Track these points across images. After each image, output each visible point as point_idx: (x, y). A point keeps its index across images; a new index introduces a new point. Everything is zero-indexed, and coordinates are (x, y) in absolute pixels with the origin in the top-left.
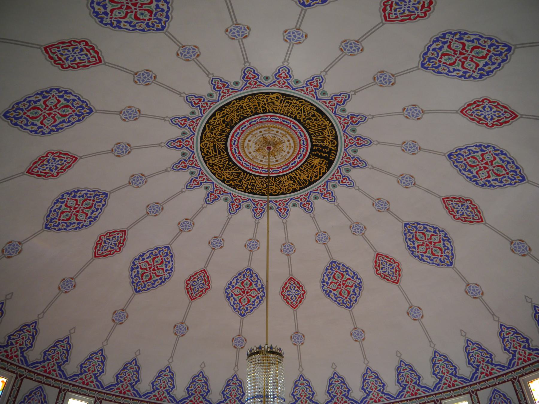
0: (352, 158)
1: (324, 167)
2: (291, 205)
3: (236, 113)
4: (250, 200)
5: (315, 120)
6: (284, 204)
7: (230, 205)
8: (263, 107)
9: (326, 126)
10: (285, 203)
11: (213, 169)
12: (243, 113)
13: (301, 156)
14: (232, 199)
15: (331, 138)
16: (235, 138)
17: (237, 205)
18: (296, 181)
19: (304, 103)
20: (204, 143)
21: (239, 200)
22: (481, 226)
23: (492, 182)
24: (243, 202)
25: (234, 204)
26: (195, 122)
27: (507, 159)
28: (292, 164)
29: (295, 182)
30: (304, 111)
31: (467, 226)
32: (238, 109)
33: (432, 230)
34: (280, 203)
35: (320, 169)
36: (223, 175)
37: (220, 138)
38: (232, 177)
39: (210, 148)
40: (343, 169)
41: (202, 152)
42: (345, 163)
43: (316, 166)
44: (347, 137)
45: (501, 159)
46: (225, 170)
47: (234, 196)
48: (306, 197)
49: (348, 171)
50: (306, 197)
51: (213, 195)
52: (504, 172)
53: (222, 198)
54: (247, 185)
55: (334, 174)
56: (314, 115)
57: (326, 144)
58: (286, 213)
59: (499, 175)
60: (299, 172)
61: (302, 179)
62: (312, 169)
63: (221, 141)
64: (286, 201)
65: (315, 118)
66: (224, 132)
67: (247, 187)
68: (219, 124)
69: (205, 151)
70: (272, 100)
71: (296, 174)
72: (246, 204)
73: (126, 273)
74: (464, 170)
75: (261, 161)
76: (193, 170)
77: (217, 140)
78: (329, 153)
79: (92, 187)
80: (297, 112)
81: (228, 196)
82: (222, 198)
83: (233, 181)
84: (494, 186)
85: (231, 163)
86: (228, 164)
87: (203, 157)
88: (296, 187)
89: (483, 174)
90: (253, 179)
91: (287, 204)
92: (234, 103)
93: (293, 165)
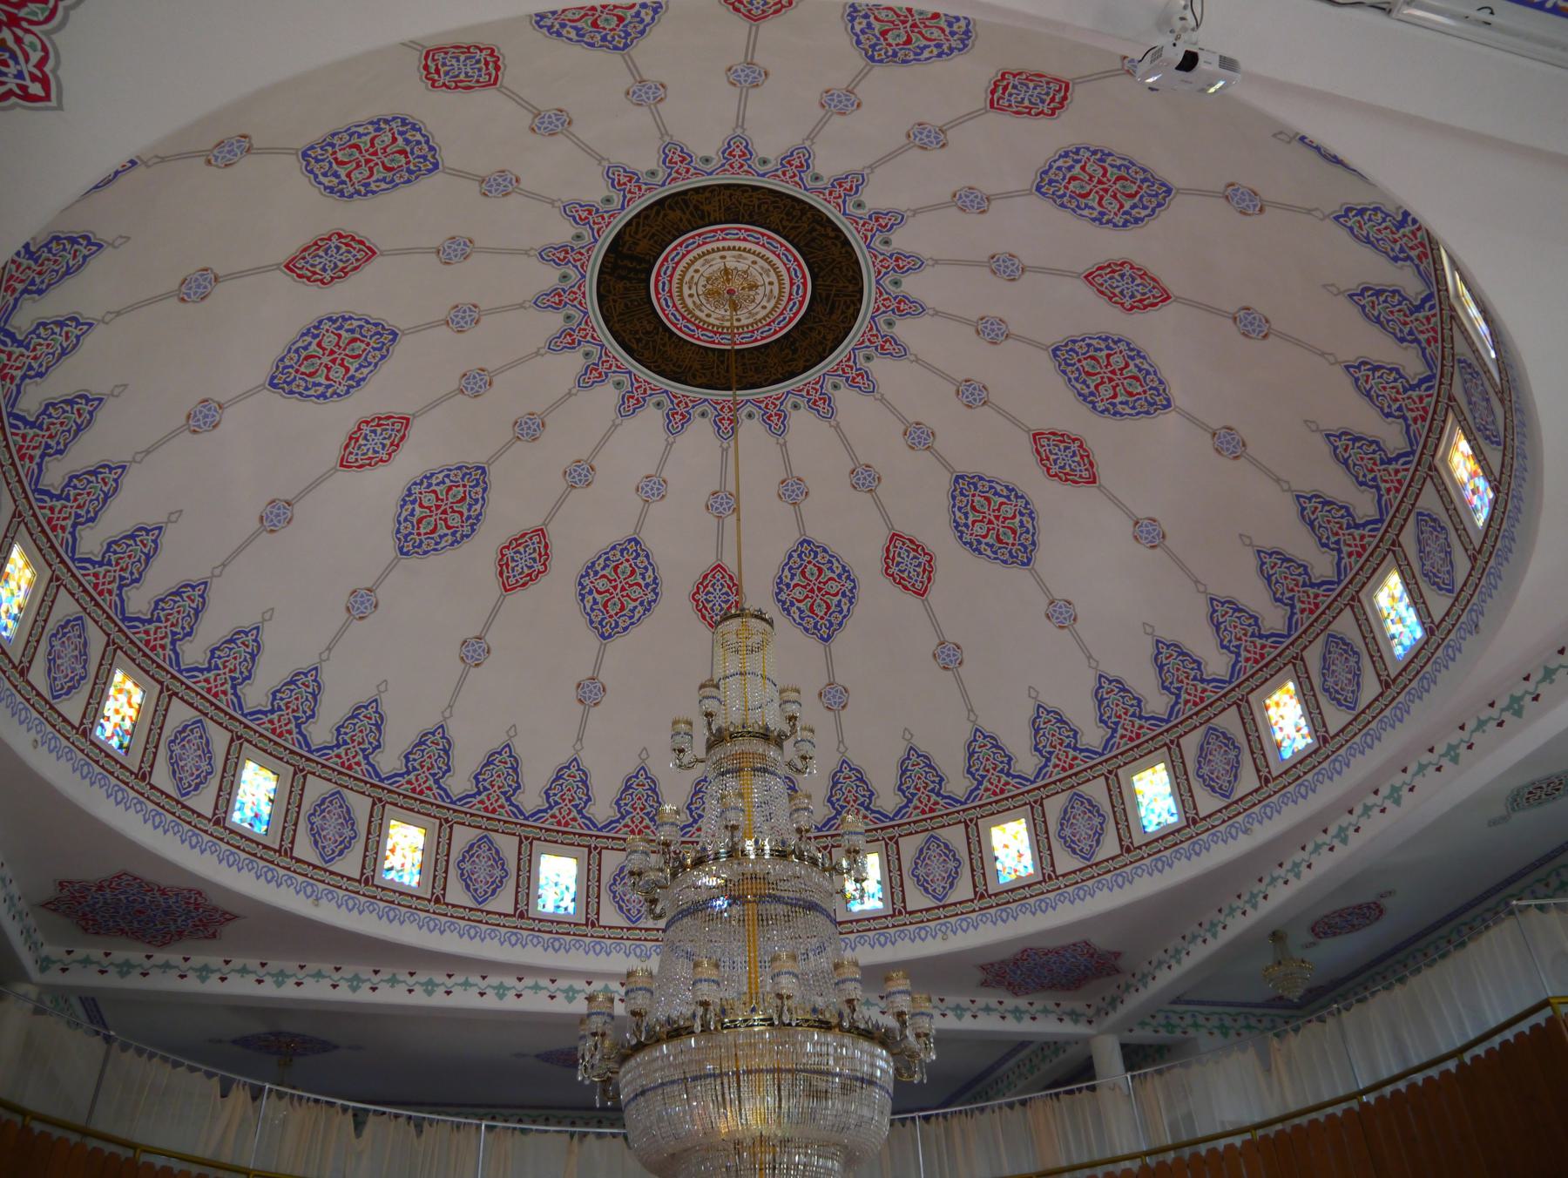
1: (627, 237)
22: (284, 257)
23: (308, 339)
26: (841, 370)
27: (311, 392)
29: (696, 207)
31: (307, 239)
33: (373, 187)
45: (320, 384)
52: (303, 369)
56: (639, 341)
59: (307, 358)
61: (679, 213)
69: (851, 311)
73: (1153, 226)
74: (361, 327)
76: (891, 288)
79: (1060, 381)
81: (850, 209)
83: (826, 236)
84: (304, 335)
89: (329, 341)
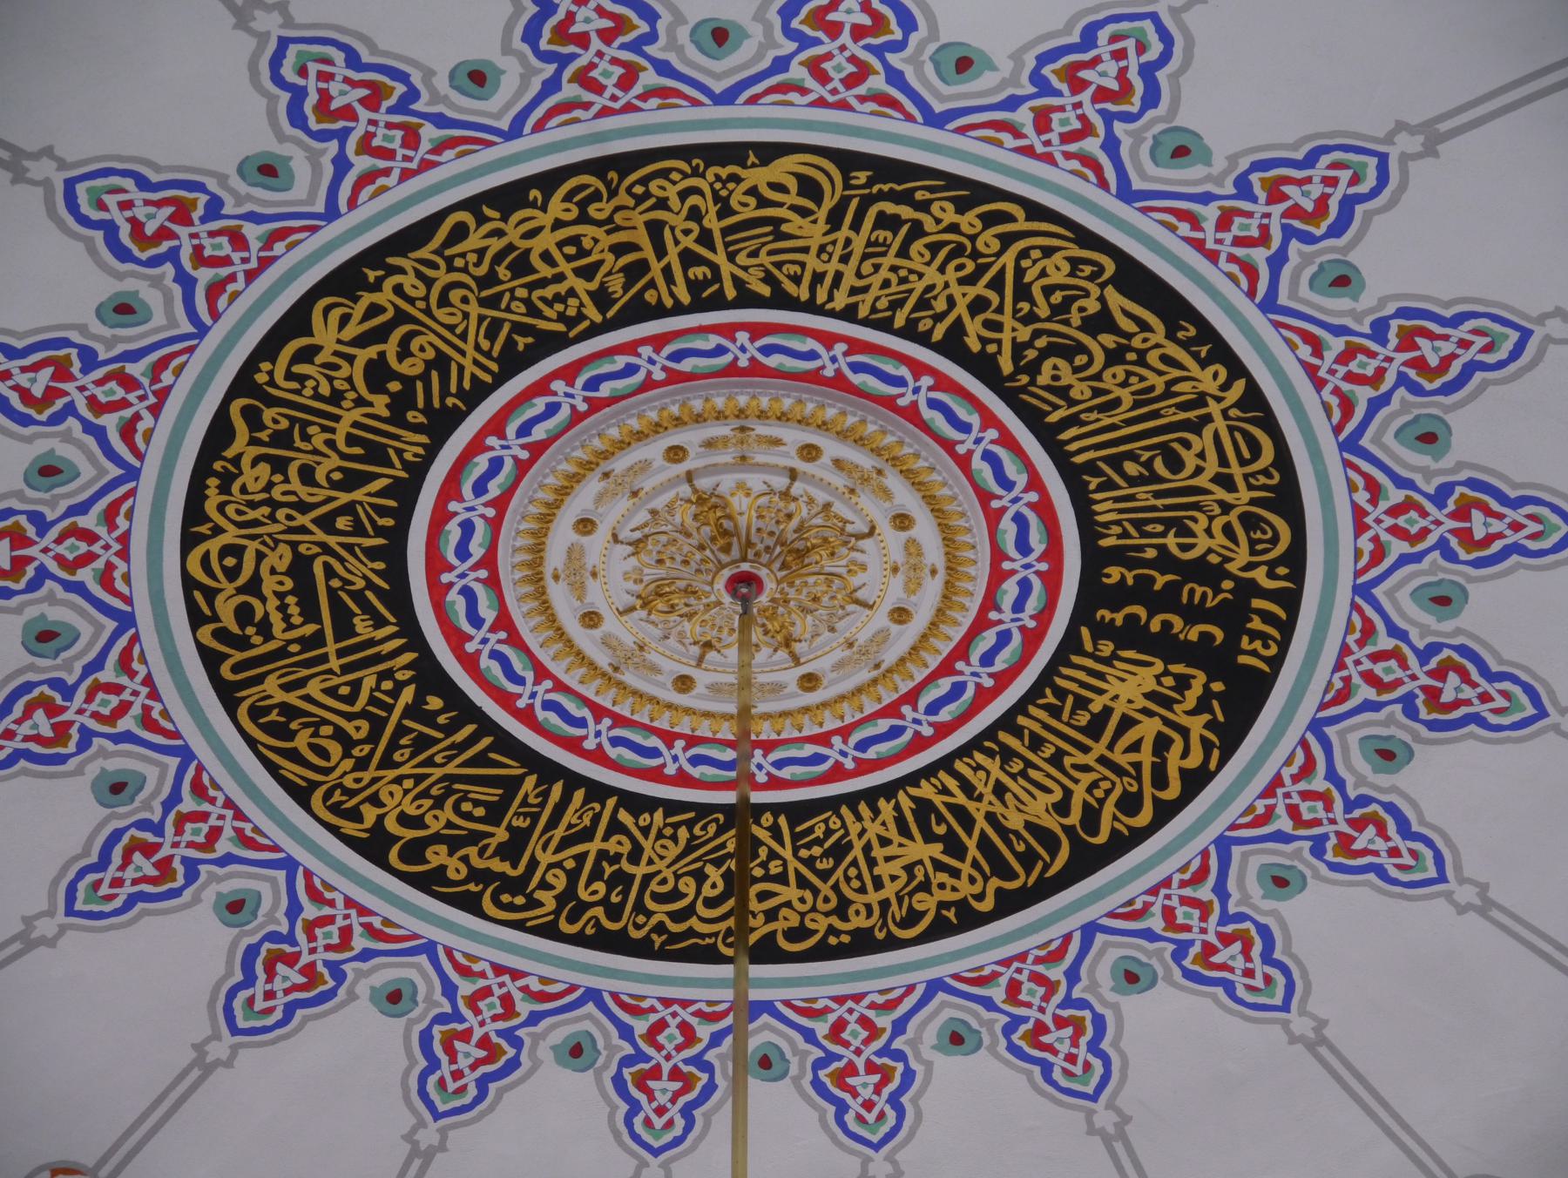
0: (1424, 655)
1: (1196, 725)
2: (931, 1035)
3: (474, 309)
4: (593, 995)
5: (1114, 357)
6: (874, 1032)
7: (426, 1038)
8: (688, 258)
9: (1201, 400)
10: (884, 1021)
11: (294, 756)
12: (533, 311)
13: (1004, 638)
14: (449, 990)
15: (1245, 495)
16: (470, 506)
17: (484, 1042)
18: (971, 844)
19: (1022, 225)
20: (214, 546)
21: (507, 1001)
24: (534, 1019)
25: (466, 1036)
26: (140, 379)
28: (933, 708)
29: (955, 847)
30: (1022, 292)
32: (490, 279)
34: (840, 1026)
35: (1162, 744)
36: (375, 800)
37: (349, 509)
38: (447, 813)
39: (269, 585)
40: (1350, 740)
41: (196, 619)
42: (1366, 692)
43: (1127, 723)
44: (1374, 488)
46: (387, 763)
47: (465, 972)
48: (1056, 973)
49: (1387, 755)
50: (1056, 973)
51: (291, 960)
53: (363, 989)
54: (573, 876)
55: (1277, 781)
56: (1101, 322)
57: (1203, 543)
58: (894, 1100)
60: (993, 766)
61: (1015, 821)
62: (1100, 748)
63: (359, 530)
64: (890, 1006)
65: (1109, 340)
66: (376, 454)
67: (569, 894)
68: (336, 398)
70: (763, 202)
71: (967, 788)
72: (560, 1031)
75: (684, 683)
76: (123, 761)
77: (326, 523)
78: (1233, 615)
80: (964, 297)
81: (416, 973)
82: (363, 989)
83: (454, 844)
85: (435, 703)
86: (413, 711)
87: (211, 660)
88: (965, 889)
90: (616, 827)
91: (899, 1027)
92: (460, 232)
93: (945, 715)
